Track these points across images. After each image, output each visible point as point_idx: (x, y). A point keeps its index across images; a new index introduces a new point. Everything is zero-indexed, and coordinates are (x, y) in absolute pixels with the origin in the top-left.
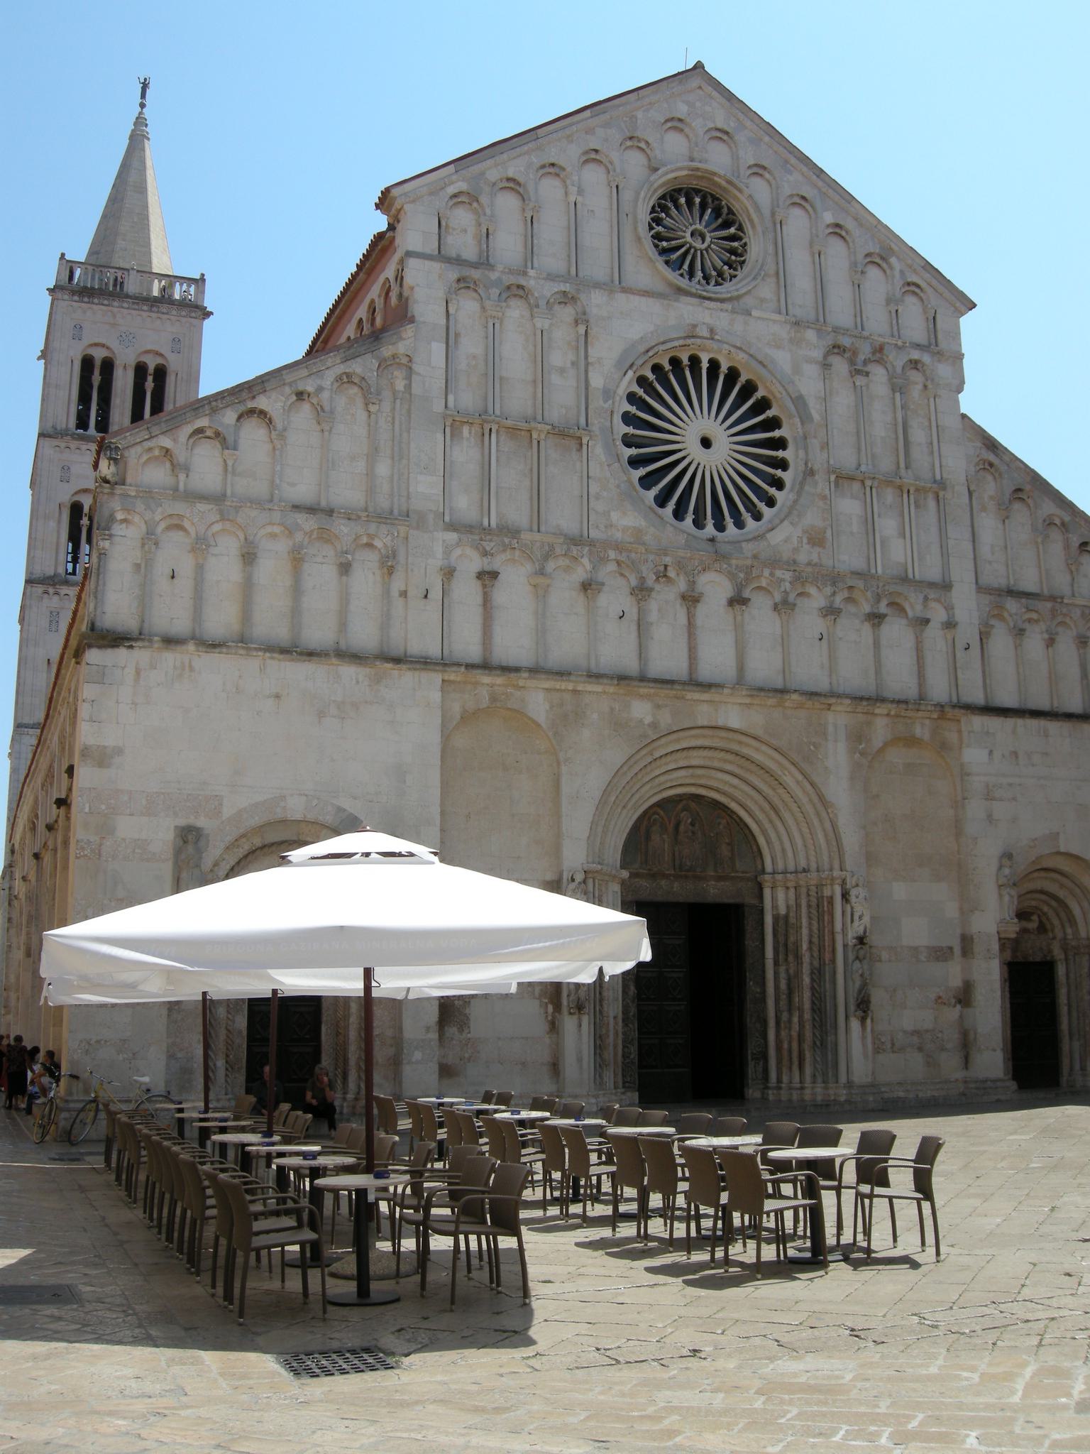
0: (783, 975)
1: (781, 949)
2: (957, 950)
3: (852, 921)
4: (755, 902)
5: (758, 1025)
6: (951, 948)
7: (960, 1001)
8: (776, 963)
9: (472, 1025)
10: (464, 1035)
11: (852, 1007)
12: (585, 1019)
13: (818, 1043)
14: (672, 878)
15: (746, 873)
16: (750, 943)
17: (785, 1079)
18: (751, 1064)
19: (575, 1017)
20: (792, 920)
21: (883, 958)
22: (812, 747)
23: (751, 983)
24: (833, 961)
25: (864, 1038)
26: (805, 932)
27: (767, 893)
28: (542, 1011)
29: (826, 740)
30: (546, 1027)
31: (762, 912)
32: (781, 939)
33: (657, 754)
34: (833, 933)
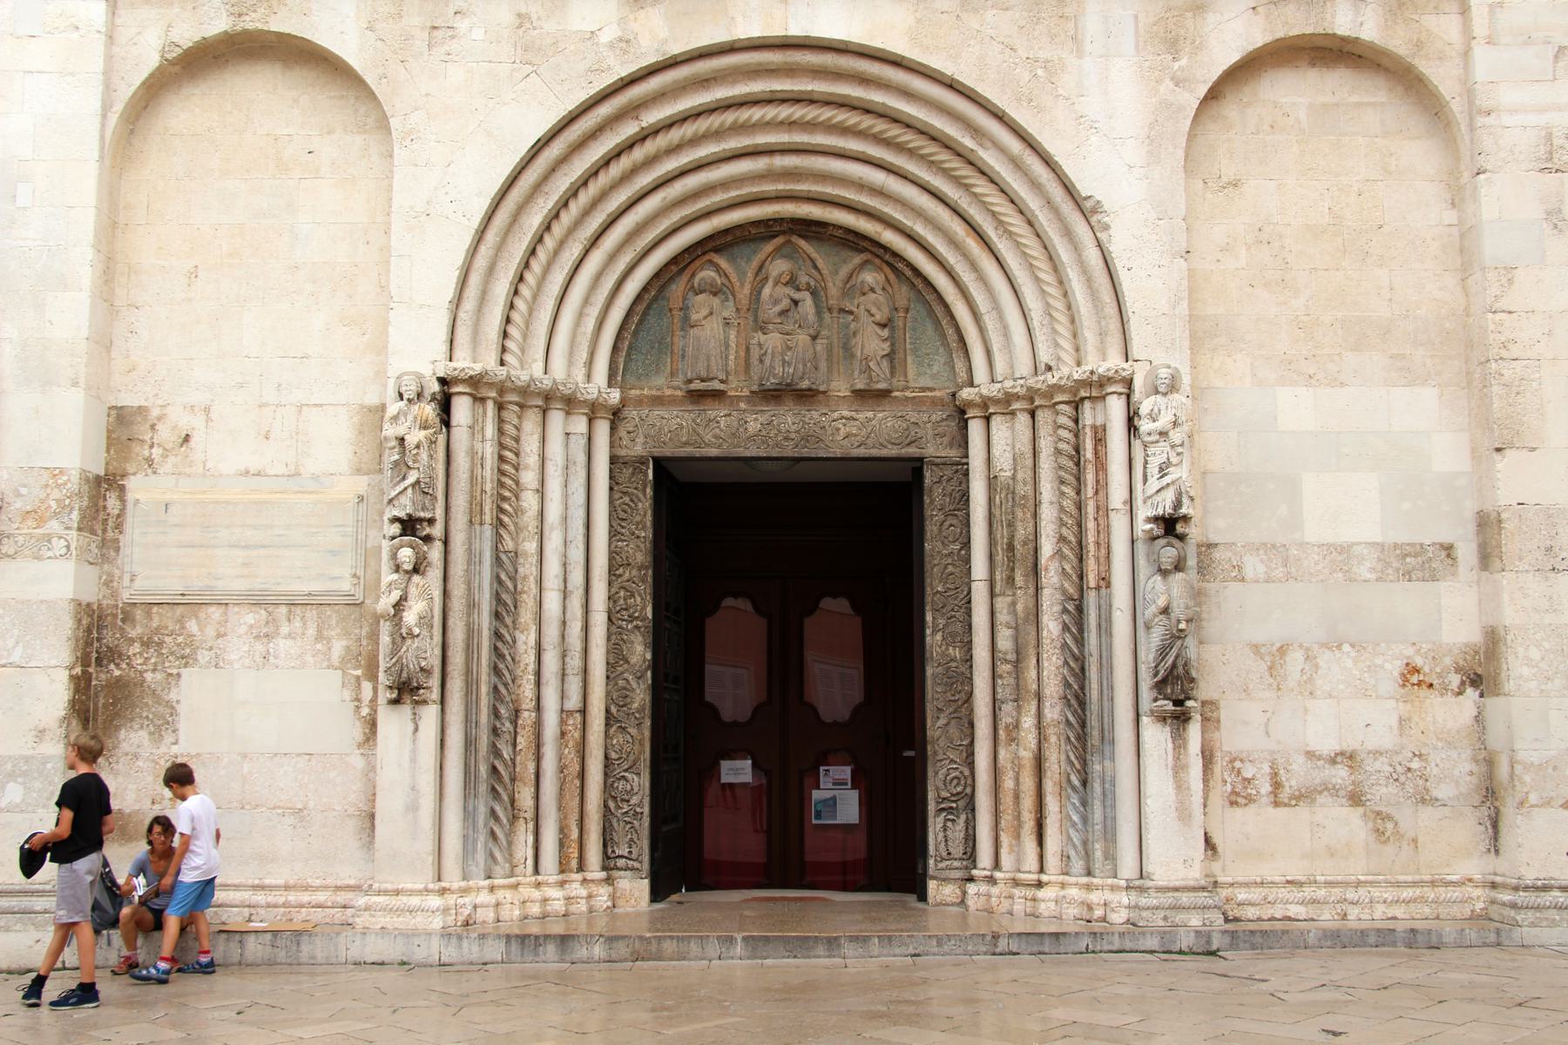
0: (1003, 617)
1: (1000, 557)
2: (1467, 552)
3: (1145, 480)
4: (953, 453)
5: (953, 730)
6: (1448, 549)
7: (1476, 681)
8: (992, 595)
9: (183, 725)
10: (163, 749)
11: (1146, 694)
12: (430, 713)
13: (1075, 781)
14: (743, 405)
15: (931, 389)
16: (935, 547)
17: (1006, 860)
18: (935, 825)
19: (406, 710)
20: (1024, 489)
21: (1249, 572)
22: (1040, 72)
23: (939, 637)
24: (1105, 581)
25: (1179, 768)
26: (1048, 513)
27: (975, 429)
28: (347, 694)
29: (1080, 54)
30: (358, 732)
31: (962, 471)
32: (1002, 534)
33: (652, 117)
34: (1103, 510)
